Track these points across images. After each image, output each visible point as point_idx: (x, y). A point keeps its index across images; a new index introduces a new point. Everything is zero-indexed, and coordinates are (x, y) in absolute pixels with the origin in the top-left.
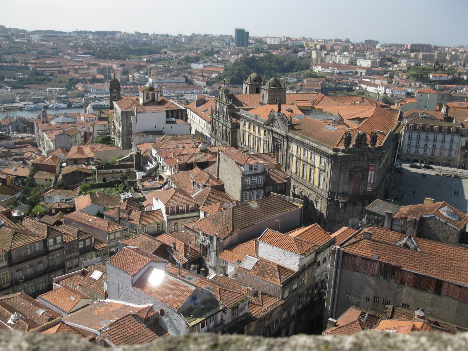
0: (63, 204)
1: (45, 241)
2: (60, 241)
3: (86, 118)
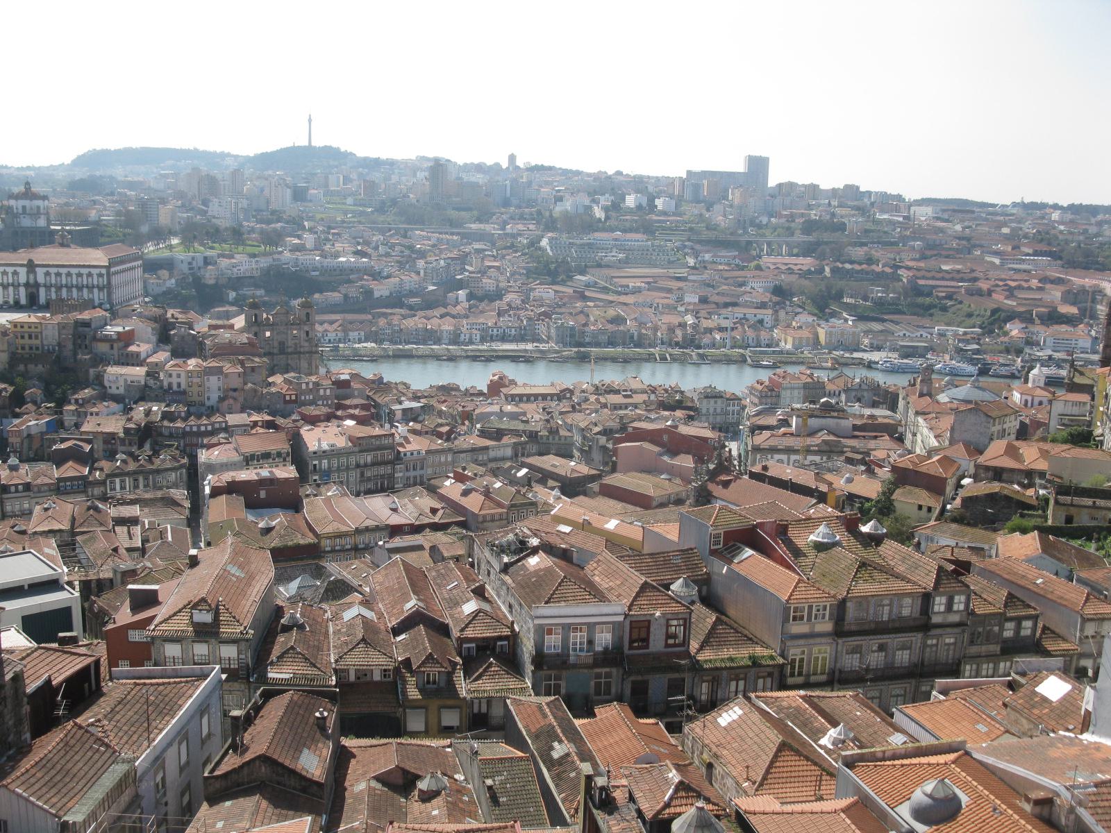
0: (962, 551)
1: (927, 598)
2: (962, 607)
3: (1025, 397)
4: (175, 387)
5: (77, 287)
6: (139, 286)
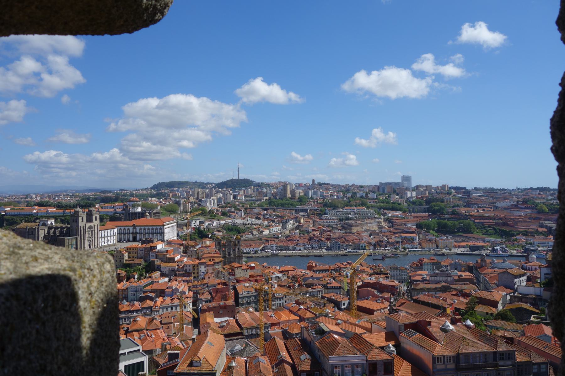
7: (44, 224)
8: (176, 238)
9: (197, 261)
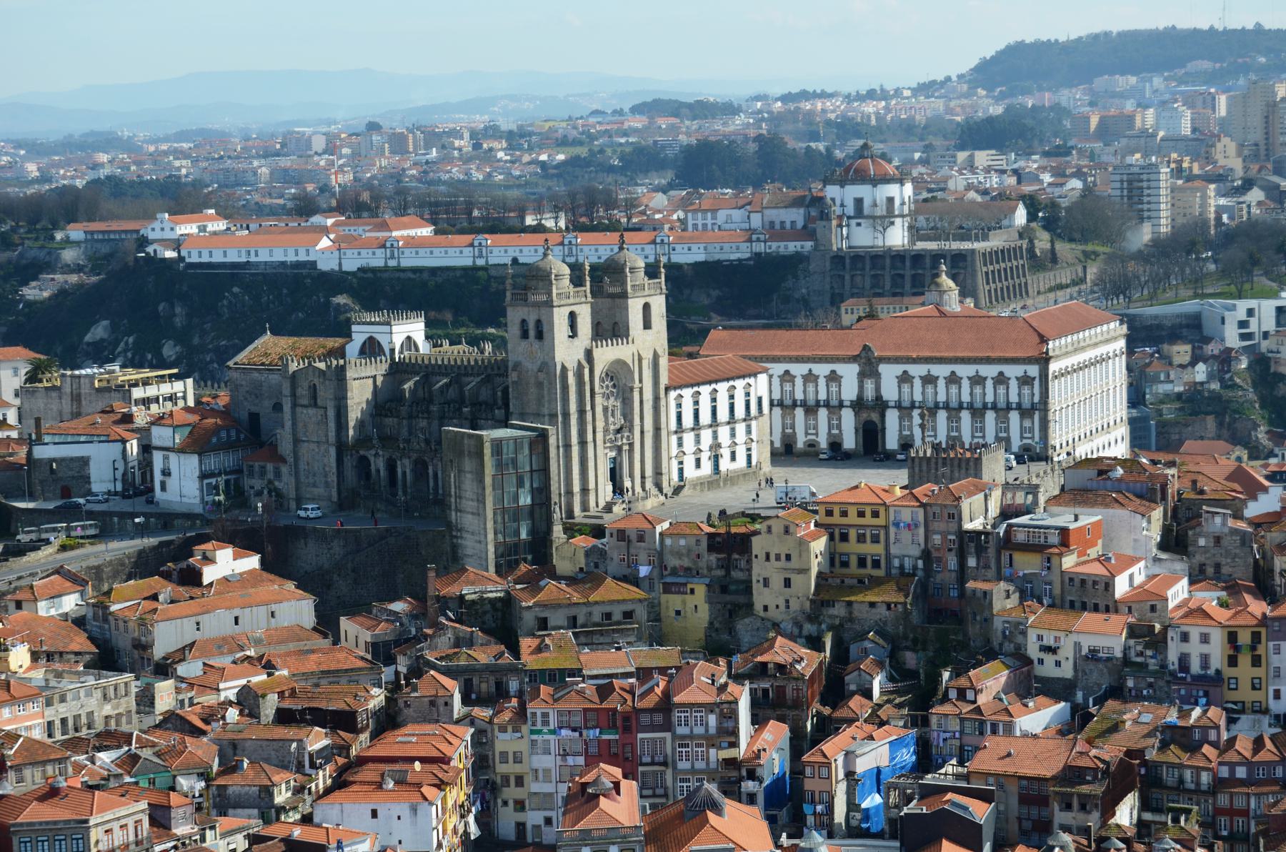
4: (1195, 667)
5: (971, 407)
6: (1118, 408)
7: (371, 349)
8: (1116, 445)
9: (1258, 607)
